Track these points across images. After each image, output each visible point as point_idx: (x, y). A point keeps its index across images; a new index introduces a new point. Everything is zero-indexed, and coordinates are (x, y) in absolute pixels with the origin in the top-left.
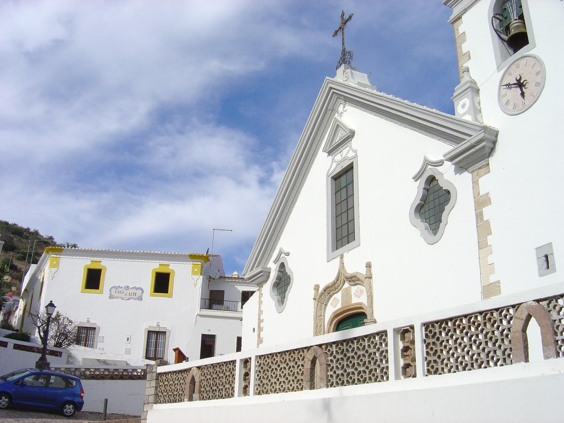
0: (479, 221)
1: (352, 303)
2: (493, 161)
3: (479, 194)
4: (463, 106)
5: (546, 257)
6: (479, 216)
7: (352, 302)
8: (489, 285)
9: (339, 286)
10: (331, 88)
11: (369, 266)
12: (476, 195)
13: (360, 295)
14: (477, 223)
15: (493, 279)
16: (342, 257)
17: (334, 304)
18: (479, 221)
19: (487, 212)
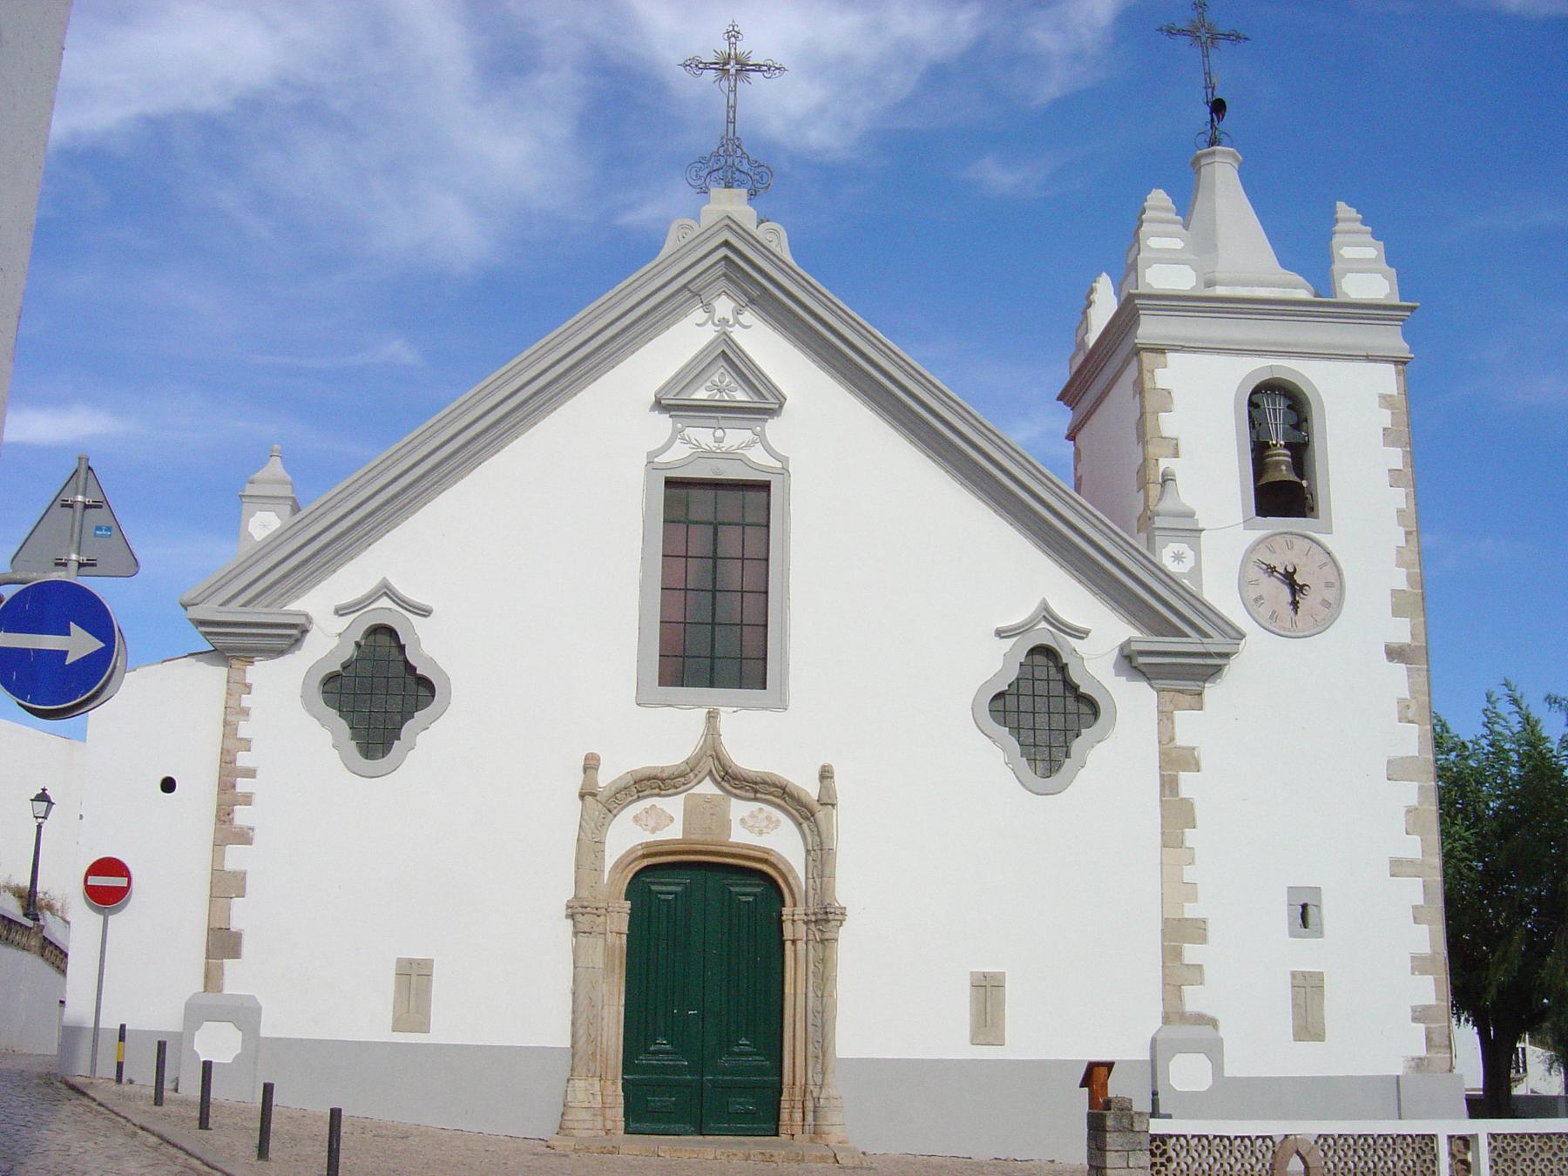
0: (1167, 793)
1: (730, 840)
2: (1211, 691)
3: (1172, 739)
4: (1178, 557)
5: (1304, 907)
6: (1169, 785)
7: (730, 836)
8: (1179, 920)
9: (684, 784)
10: (726, 244)
11: (825, 775)
12: (1166, 739)
13: (765, 830)
14: (1162, 794)
15: (1191, 911)
16: (712, 717)
17: (652, 823)
18: (1167, 793)
19: (1188, 783)
